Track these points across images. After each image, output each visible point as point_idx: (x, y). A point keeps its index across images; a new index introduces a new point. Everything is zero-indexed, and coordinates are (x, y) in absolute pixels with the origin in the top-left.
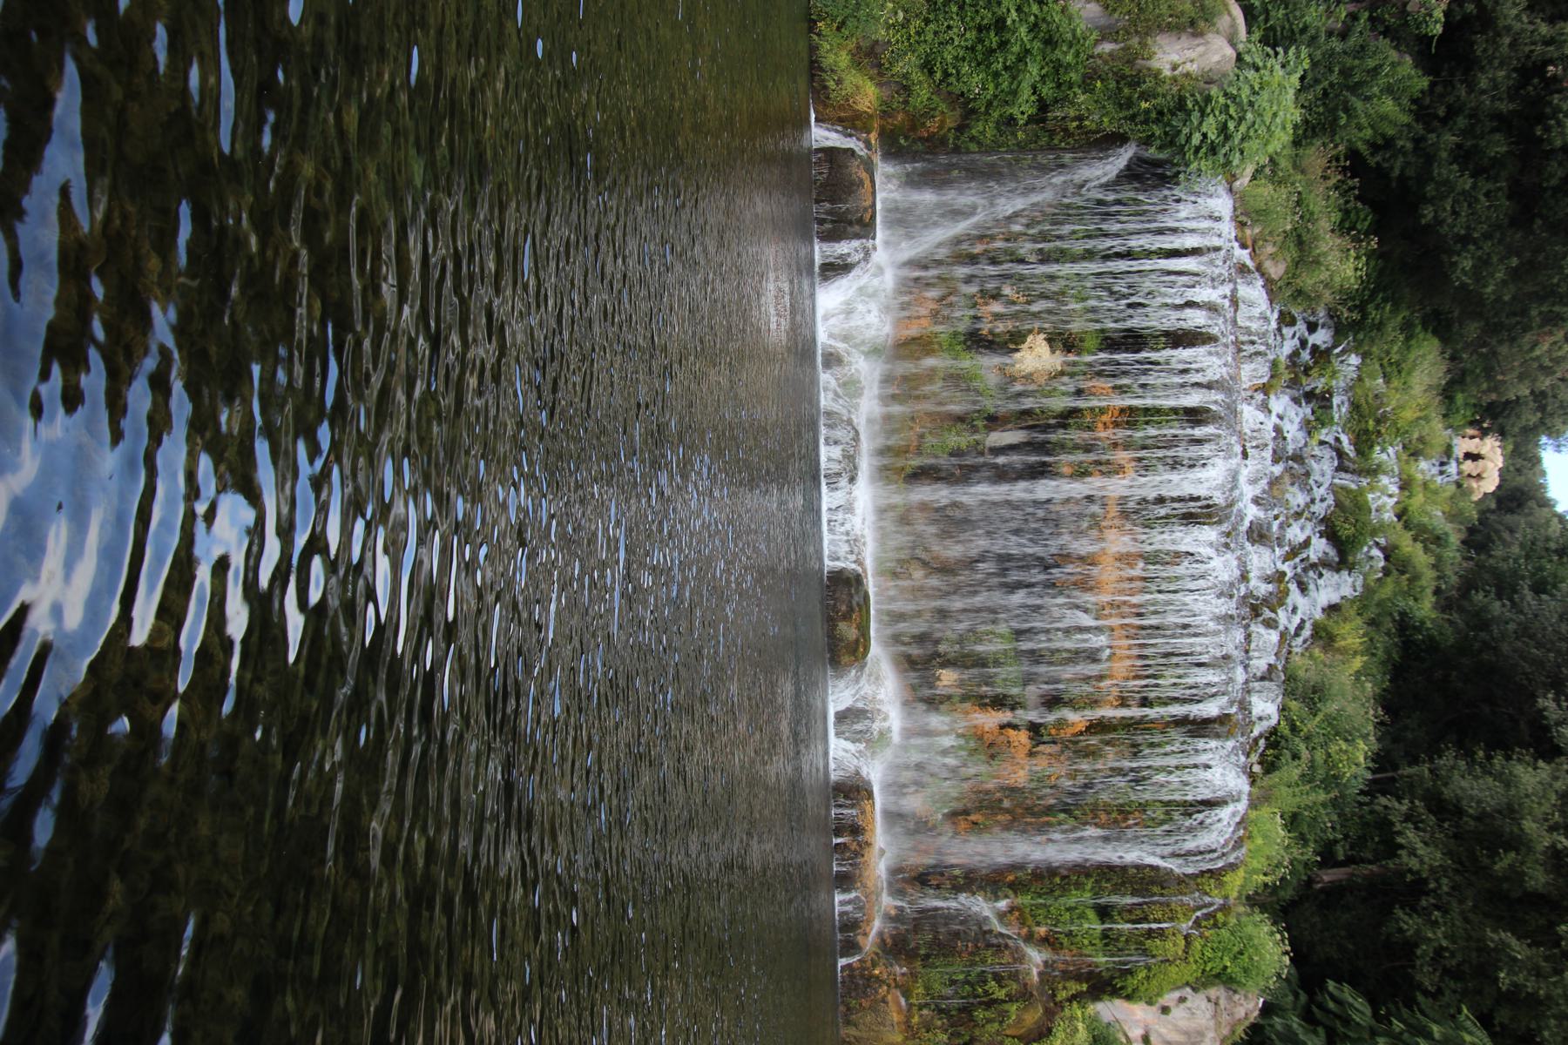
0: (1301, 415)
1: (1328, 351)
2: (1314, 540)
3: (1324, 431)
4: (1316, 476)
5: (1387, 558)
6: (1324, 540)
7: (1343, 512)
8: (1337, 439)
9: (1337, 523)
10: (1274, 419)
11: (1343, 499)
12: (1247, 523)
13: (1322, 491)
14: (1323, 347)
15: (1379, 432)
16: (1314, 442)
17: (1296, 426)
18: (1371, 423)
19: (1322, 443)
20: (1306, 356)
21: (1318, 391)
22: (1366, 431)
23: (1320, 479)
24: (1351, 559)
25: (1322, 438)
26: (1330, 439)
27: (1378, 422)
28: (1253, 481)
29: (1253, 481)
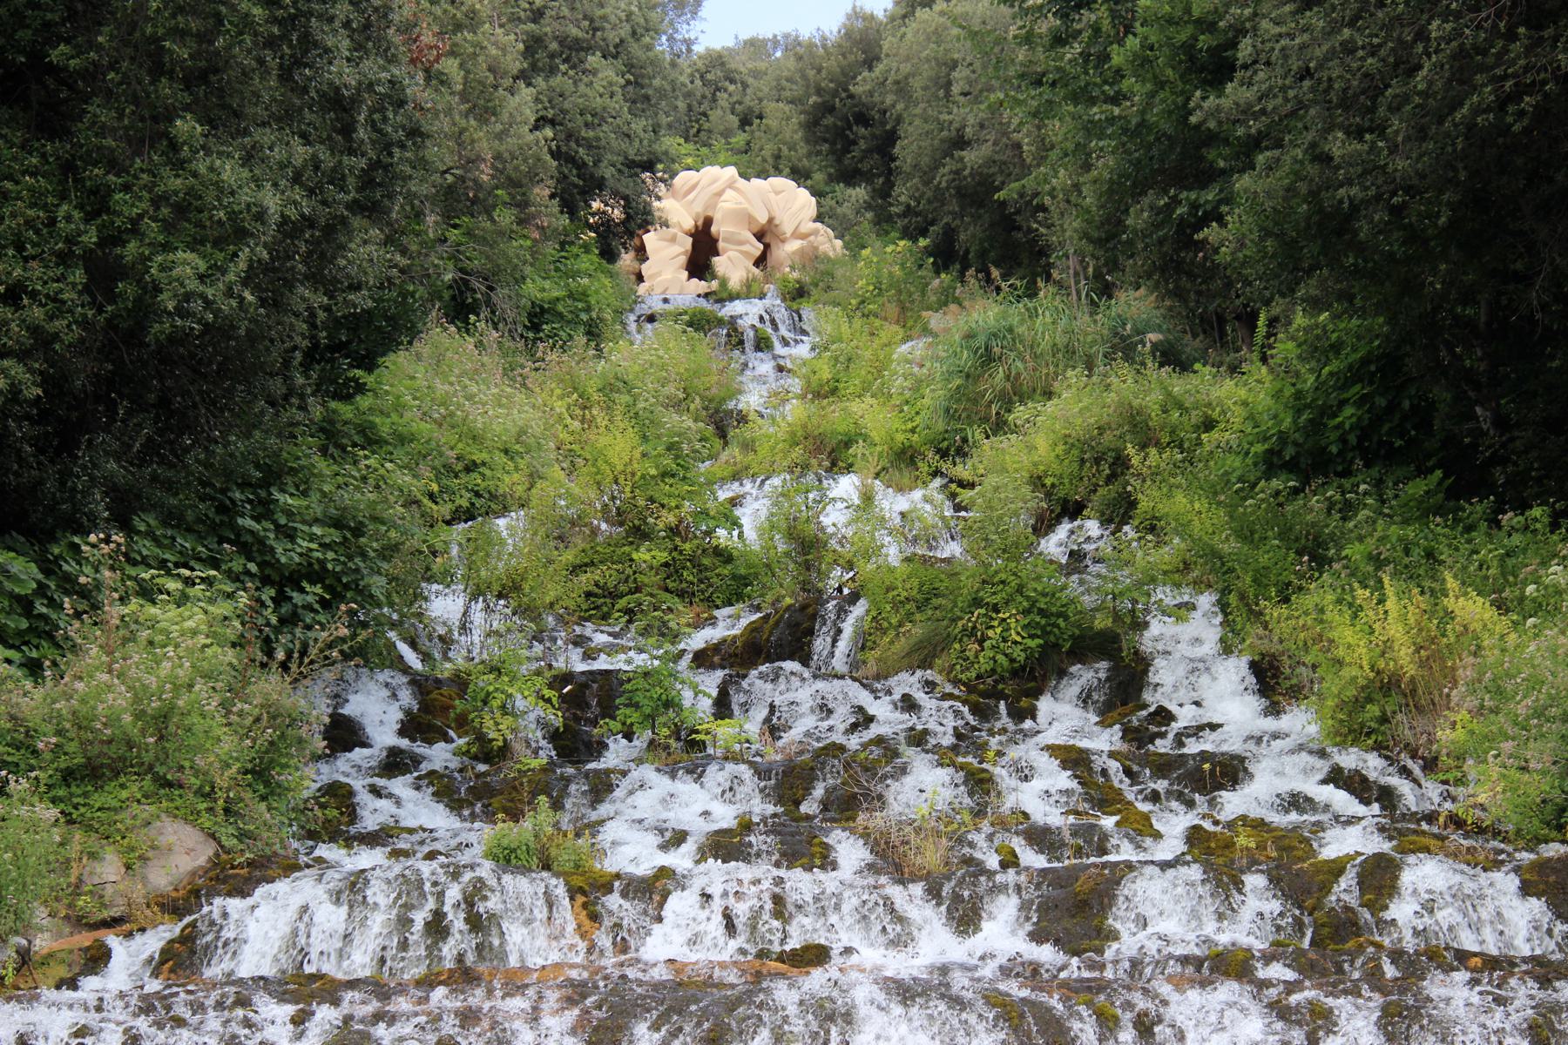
0: (648, 772)
1: (420, 684)
2: (1052, 736)
3: (687, 696)
4: (837, 727)
5: (1073, 510)
6: (1045, 705)
7: (948, 640)
8: (702, 659)
9: (984, 664)
10: (680, 859)
11: (902, 645)
12: (1046, 954)
13: (880, 709)
14: (407, 697)
15: (674, 531)
16: (725, 731)
17: (685, 787)
18: (643, 555)
19: (722, 707)
20: (439, 756)
21: (557, 719)
22: (670, 569)
23: (841, 718)
24: (1101, 622)
25: (706, 704)
26: (711, 681)
27: (640, 534)
28: (901, 937)
29: (901, 937)
